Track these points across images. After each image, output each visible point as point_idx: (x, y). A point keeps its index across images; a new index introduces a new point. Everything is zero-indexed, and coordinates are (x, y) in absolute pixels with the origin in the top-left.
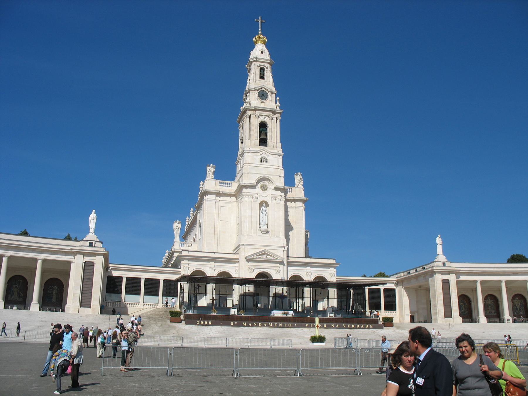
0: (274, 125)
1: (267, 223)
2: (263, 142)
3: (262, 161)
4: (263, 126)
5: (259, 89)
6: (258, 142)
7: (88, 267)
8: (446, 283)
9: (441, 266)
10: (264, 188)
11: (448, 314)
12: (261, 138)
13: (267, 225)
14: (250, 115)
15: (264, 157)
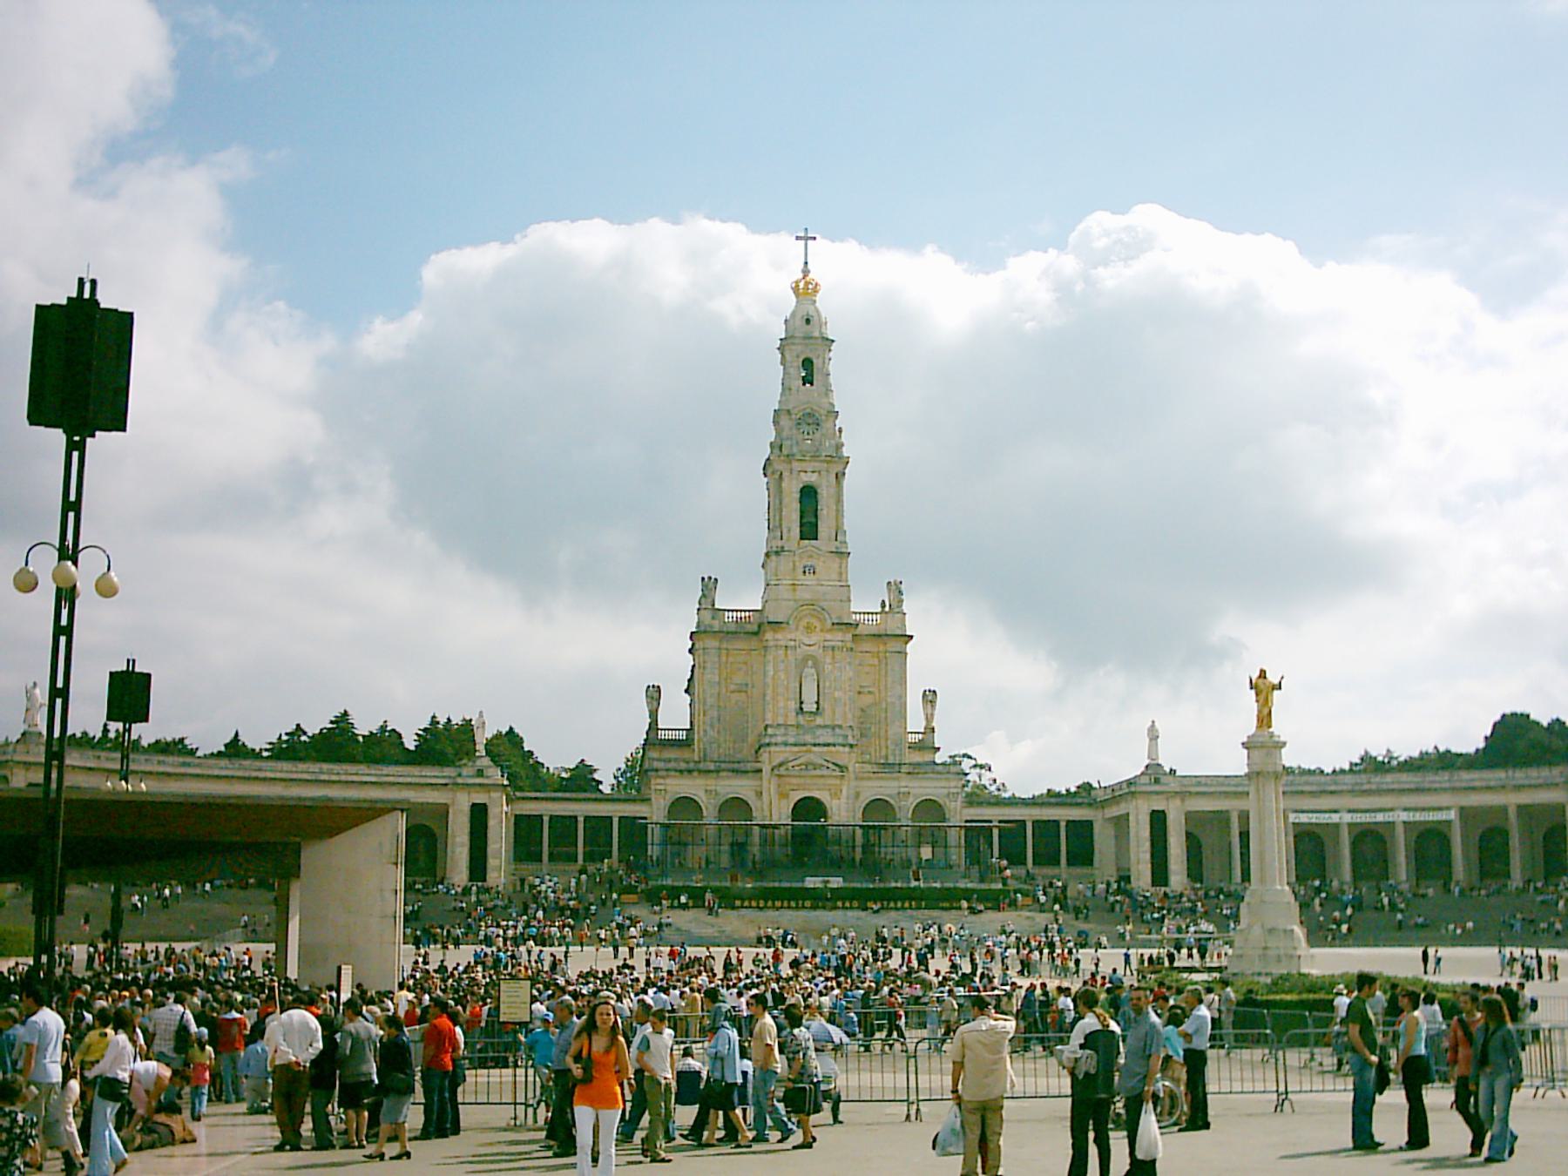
0: (833, 491)
1: (816, 699)
2: (809, 530)
3: (805, 572)
4: (809, 494)
5: (799, 411)
6: (796, 531)
7: (479, 814)
8: (1158, 820)
9: (1150, 784)
10: (809, 629)
11: (1160, 874)
12: (805, 520)
13: (817, 703)
14: (781, 474)
15: (809, 563)
